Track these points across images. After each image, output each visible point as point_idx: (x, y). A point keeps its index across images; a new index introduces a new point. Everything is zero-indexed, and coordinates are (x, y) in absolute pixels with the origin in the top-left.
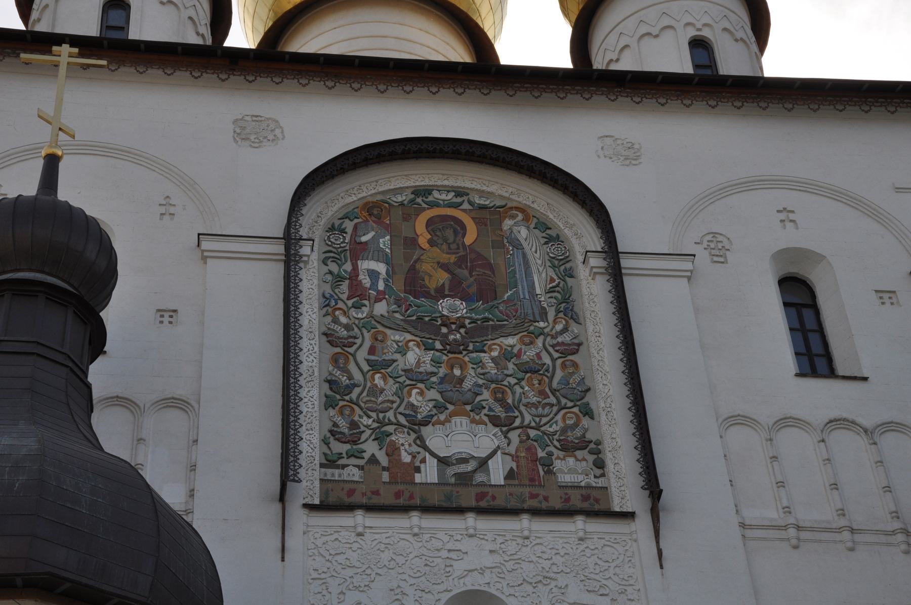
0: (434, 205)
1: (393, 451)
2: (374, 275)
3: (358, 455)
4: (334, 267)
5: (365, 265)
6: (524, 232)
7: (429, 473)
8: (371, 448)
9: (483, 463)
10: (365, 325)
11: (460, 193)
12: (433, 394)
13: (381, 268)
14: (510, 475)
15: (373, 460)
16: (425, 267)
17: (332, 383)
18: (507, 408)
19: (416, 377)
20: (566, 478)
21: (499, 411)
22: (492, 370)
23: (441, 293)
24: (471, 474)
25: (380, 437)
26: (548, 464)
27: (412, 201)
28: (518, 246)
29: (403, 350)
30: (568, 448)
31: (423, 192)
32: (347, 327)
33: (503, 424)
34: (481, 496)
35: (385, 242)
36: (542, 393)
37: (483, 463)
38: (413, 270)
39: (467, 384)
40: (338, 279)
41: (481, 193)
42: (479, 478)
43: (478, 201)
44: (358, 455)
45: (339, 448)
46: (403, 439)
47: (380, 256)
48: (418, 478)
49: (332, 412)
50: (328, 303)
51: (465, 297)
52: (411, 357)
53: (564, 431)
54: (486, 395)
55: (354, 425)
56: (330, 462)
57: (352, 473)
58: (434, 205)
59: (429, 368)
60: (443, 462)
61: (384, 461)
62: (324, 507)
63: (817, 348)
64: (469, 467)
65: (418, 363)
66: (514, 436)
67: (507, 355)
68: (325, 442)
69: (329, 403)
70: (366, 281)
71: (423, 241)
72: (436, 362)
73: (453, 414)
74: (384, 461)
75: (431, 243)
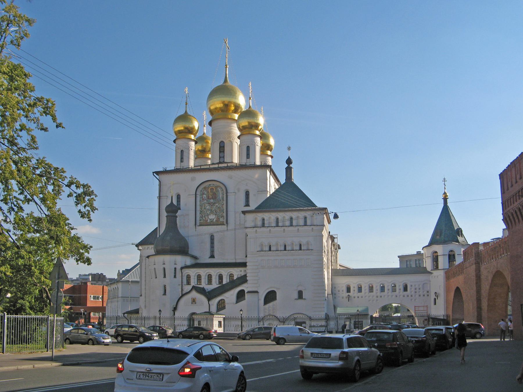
0: (211, 186)
1: (206, 218)
2: (205, 197)
3: (203, 219)
4: (201, 196)
5: (204, 196)
6: (220, 189)
7: (209, 221)
8: (204, 218)
9: (214, 219)
10: (204, 204)
11: (213, 184)
12: (210, 212)
13: (205, 196)
14: (216, 220)
15: (204, 220)
16: (209, 195)
17: (201, 211)
18: (216, 213)
19: (208, 210)
20: (221, 220)
21: (215, 213)
22: (215, 208)
23: (211, 199)
24: (212, 221)
25: (205, 217)
26: (219, 219)
27: (209, 186)
28: (219, 191)
29: (207, 207)
30: (221, 217)
31: (210, 185)
32: (202, 204)
33: (216, 215)
34: (213, 223)
35: (206, 193)
36: (220, 211)
37: (214, 219)
38: (208, 196)
39: (213, 210)
40: (201, 197)
41: (216, 185)
42: (213, 221)
43: (215, 185)
44: (203, 219)
45: (201, 218)
46: (207, 217)
47: (206, 195)
48: (208, 221)
49: (200, 214)
50: (200, 201)
51: (213, 199)
52: (208, 207)
53: (221, 215)
54: (214, 212)
55: (202, 216)
56: (200, 220)
57: (202, 221)
58: (211, 186)
59: (209, 208)
60: (210, 219)
61: (205, 220)
62: (200, 225)
63: (247, 202)
64: (212, 220)
65: (208, 208)
66: (217, 216)
67: (217, 206)
68: (200, 218)
69: (200, 213)
70: (204, 198)
71: (209, 192)
72: (210, 208)
73: (212, 214)
74: (205, 220)
75: (210, 192)
